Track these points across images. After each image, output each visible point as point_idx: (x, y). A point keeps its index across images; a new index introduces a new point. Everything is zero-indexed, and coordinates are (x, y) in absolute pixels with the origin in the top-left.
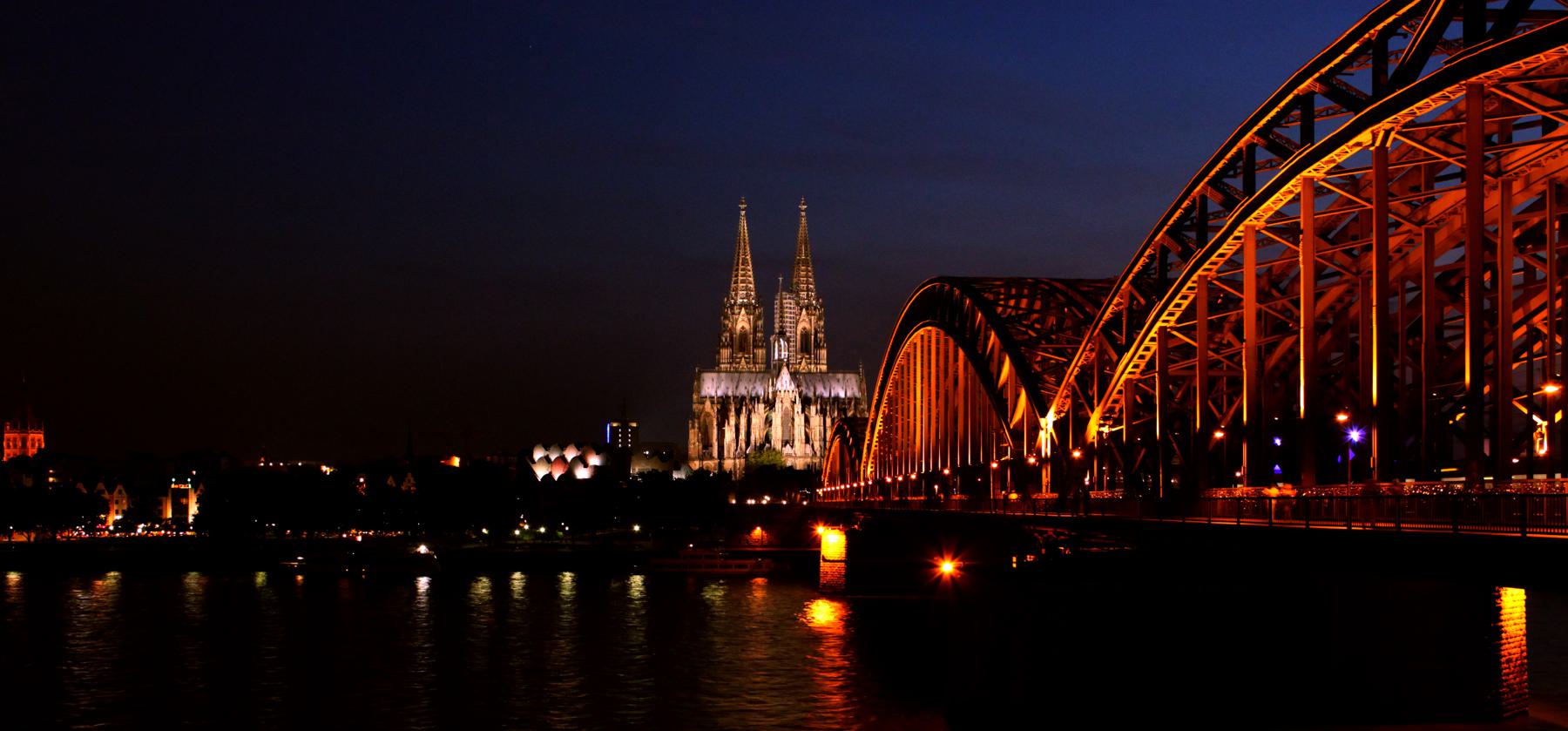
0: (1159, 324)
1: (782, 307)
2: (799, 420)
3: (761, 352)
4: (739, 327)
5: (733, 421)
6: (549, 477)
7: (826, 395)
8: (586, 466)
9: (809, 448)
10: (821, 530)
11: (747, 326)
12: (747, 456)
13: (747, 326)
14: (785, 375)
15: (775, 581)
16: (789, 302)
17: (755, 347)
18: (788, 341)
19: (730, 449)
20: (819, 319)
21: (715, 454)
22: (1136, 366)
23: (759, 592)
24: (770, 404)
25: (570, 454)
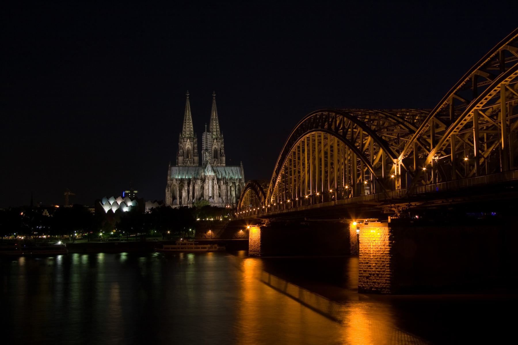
0: (475, 108)
1: (207, 139)
2: (216, 187)
3: (196, 158)
4: (187, 147)
5: (186, 188)
6: (110, 211)
7: (227, 177)
8: (127, 206)
9: (220, 200)
10: (248, 227)
11: (190, 147)
12: (193, 203)
13: (190, 147)
14: (209, 167)
15: (218, 253)
16: (209, 137)
17: (194, 156)
18: (209, 153)
19: (185, 199)
20: (222, 144)
21: (178, 203)
22: (458, 129)
23: (210, 257)
24: (203, 180)
25: (119, 202)
